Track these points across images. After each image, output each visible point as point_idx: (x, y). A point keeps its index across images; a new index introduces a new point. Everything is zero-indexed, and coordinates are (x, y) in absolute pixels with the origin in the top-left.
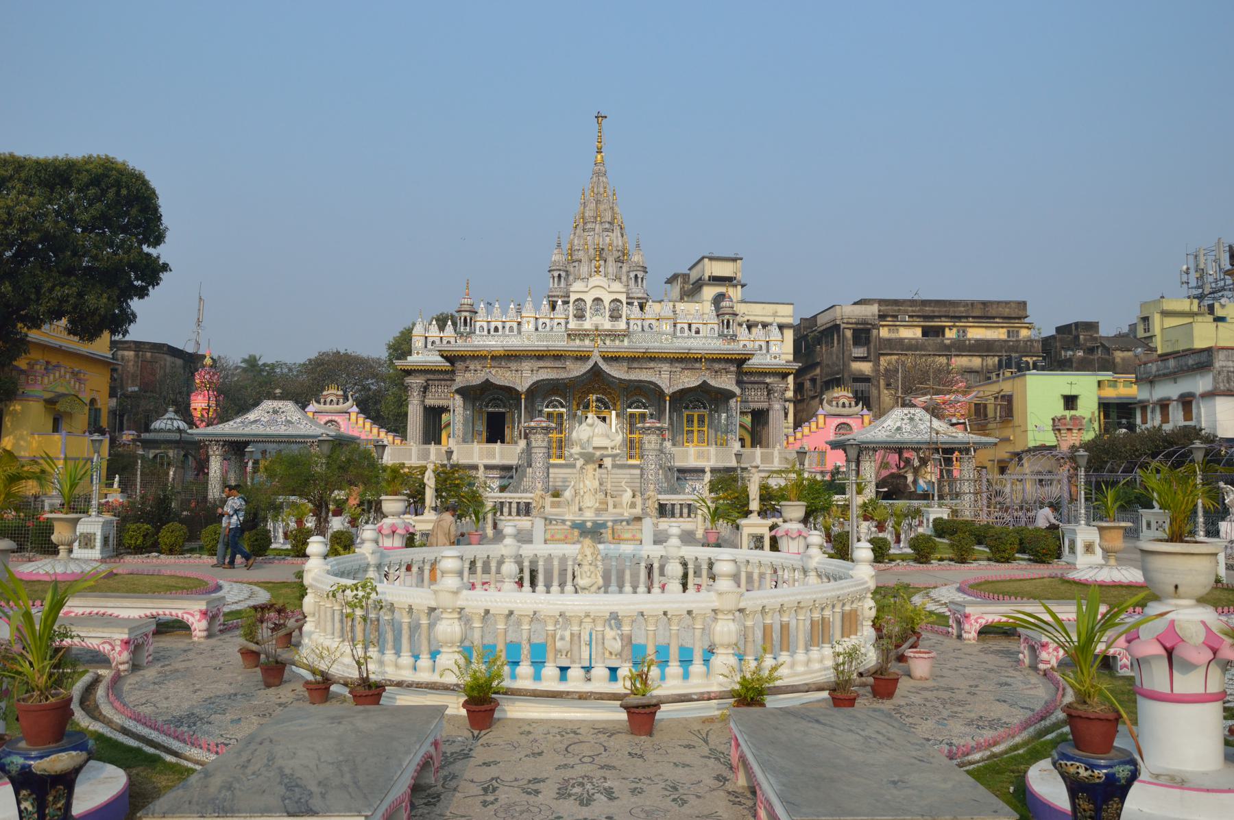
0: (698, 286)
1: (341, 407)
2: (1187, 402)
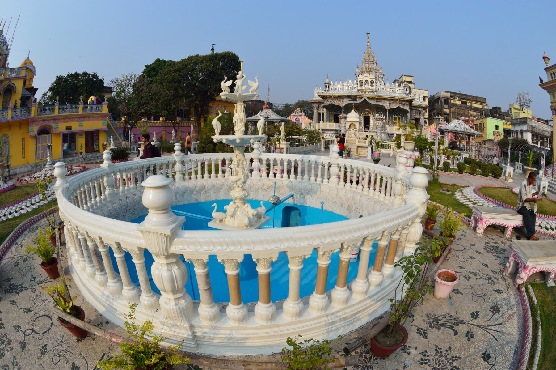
1: (300, 114)
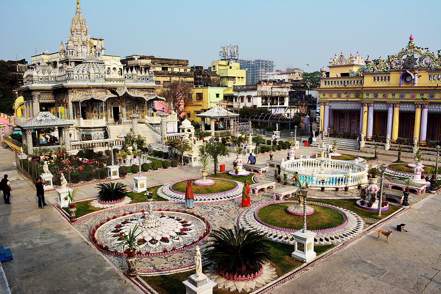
2: (249, 98)
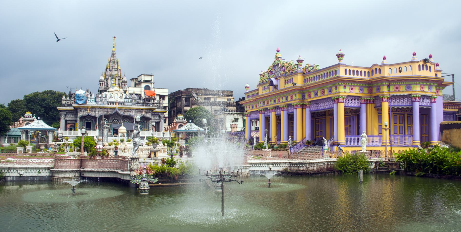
0: (140, 83)
